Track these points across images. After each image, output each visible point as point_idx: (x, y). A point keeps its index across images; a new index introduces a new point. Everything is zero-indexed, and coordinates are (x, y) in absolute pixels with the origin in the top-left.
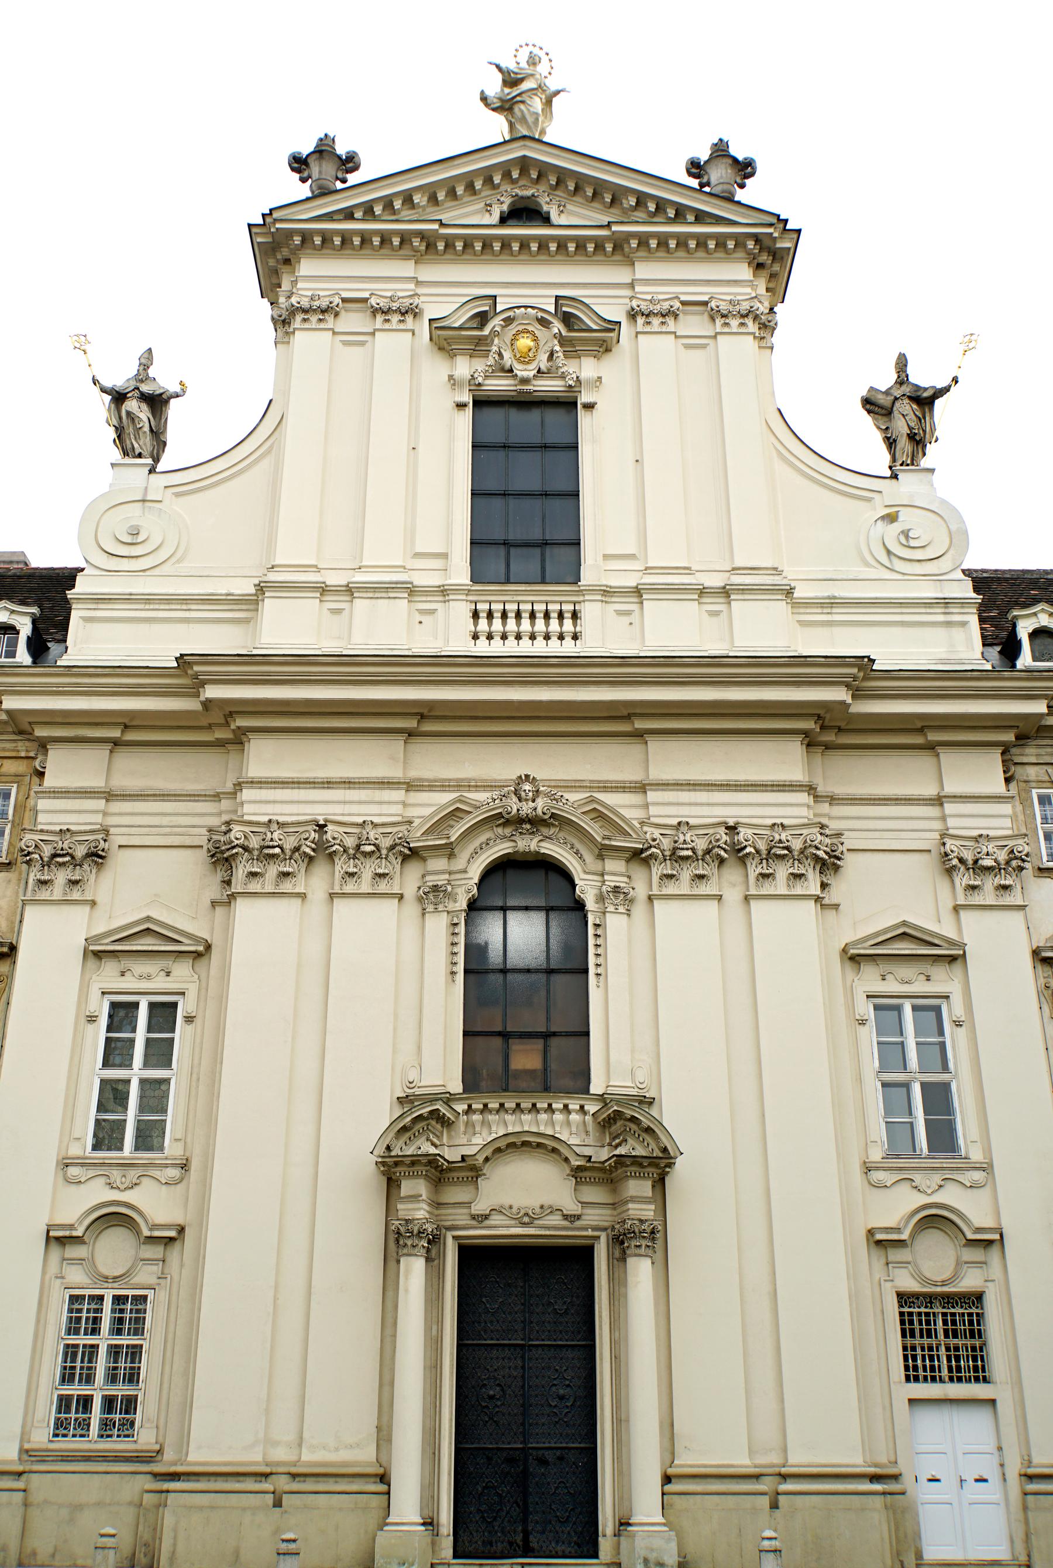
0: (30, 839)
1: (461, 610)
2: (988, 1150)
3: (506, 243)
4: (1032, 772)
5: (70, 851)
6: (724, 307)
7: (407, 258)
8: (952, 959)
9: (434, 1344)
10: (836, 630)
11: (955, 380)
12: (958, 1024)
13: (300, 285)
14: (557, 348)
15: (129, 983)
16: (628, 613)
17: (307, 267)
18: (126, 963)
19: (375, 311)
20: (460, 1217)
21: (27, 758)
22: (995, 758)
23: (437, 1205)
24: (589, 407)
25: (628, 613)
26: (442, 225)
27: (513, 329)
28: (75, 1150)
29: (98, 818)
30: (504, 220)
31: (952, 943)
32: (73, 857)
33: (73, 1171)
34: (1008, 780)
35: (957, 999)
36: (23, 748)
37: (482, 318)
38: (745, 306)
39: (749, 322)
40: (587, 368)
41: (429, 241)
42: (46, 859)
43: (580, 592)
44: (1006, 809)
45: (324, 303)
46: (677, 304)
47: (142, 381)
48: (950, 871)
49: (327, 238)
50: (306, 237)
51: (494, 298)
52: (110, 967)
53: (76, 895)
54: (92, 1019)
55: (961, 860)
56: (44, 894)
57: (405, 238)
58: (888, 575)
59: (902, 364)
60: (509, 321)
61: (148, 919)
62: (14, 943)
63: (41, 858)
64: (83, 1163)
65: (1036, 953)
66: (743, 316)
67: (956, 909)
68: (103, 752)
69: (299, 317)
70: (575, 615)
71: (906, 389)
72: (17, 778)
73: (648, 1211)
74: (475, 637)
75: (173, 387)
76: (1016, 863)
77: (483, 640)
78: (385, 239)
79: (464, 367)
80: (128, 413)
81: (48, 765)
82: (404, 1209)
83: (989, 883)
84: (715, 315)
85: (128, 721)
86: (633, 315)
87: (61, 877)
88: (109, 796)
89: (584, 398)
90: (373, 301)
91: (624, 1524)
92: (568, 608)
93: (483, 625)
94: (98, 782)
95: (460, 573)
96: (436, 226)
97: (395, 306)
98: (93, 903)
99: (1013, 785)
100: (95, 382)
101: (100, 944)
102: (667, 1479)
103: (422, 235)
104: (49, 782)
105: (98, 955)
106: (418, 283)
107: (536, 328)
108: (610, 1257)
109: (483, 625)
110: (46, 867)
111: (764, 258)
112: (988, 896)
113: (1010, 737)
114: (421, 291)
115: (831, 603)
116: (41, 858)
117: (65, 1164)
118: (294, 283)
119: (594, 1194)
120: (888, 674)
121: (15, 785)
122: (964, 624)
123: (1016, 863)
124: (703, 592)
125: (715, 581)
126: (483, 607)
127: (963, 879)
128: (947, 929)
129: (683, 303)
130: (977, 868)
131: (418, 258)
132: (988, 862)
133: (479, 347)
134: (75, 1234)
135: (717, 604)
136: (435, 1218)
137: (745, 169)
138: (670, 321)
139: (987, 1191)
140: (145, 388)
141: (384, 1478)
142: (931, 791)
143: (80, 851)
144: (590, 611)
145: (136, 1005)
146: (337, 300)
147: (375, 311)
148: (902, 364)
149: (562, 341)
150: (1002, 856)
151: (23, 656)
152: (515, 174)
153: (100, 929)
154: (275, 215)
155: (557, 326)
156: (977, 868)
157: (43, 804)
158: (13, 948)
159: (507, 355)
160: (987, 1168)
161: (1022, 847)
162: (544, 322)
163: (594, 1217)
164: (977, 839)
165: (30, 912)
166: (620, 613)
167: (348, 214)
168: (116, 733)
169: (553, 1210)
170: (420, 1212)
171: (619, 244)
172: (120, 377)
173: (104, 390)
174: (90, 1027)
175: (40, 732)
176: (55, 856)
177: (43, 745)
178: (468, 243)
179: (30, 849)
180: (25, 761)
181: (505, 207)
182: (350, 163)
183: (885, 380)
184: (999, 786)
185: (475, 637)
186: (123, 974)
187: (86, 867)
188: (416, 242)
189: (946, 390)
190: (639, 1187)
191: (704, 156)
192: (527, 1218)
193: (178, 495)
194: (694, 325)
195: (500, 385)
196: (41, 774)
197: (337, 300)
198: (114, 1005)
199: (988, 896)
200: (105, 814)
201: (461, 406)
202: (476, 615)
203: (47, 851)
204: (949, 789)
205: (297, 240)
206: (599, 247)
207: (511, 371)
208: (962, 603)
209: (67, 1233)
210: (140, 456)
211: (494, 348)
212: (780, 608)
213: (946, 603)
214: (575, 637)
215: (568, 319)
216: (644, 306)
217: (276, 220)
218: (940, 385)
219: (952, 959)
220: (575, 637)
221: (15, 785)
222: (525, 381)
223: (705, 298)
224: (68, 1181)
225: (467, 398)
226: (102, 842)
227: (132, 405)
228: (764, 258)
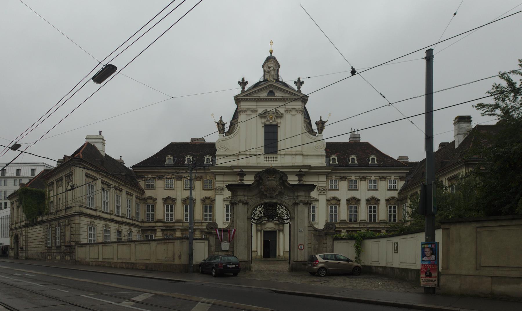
1: (262, 158)
2: (318, 221)
3: (268, 99)
4: (330, 177)
6: (298, 109)
7: (255, 101)
8: (317, 201)
9: (261, 240)
10: (308, 159)
11: (327, 121)
12: (317, 208)
13: (241, 106)
14: (275, 118)
16: (283, 157)
17: (242, 103)
19: (252, 111)
20: (264, 228)
22: (325, 176)
23: (261, 227)
24: (279, 127)
25: (283, 157)
26: (260, 97)
27: (269, 115)
28: (224, 221)
30: (268, 93)
31: (317, 199)
33: (224, 223)
34: (326, 179)
35: (317, 205)
37: (265, 113)
38: (300, 109)
39: (301, 112)
40: (279, 120)
41: (258, 99)
43: (278, 155)
44: (325, 183)
45: (244, 110)
46: (291, 109)
47: (221, 121)
48: (318, 190)
49: (244, 99)
50: (242, 99)
51: (267, 110)
52: (226, 202)
53: (221, 194)
54: (224, 207)
55: (320, 189)
56: (218, 193)
57: (255, 99)
58: (315, 151)
59: (321, 117)
60: (269, 113)
64: (225, 223)
65: (327, 200)
66: (300, 111)
67: (318, 195)
68: (222, 176)
69: (241, 112)
70: (277, 158)
71: (321, 122)
72: (212, 179)
73: (282, 228)
74: (265, 161)
75: (225, 123)
76: (325, 190)
77: (266, 161)
78: (252, 99)
79: (264, 120)
80: (220, 127)
82: (258, 228)
83: (322, 192)
84: (297, 111)
85: (225, 172)
86: (285, 111)
87: (219, 191)
88: (223, 182)
89: (279, 125)
90: (251, 109)
91: (279, 256)
92: (276, 157)
93: (266, 159)
94: (222, 180)
95: (263, 152)
96: (259, 97)
97: (254, 110)
98: (223, 194)
99: (327, 179)
100: (215, 122)
102: (284, 252)
103: (257, 98)
104: (217, 180)
105: (224, 200)
106: (257, 106)
107: (273, 115)
108: (278, 232)
109: (266, 159)
111: (304, 100)
112: (322, 194)
113: (327, 174)
114: (258, 107)
115: (307, 155)
117: (224, 223)
118: (240, 106)
119: (276, 226)
120: (313, 167)
122: (323, 158)
123: (325, 190)
124: (292, 155)
125: (294, 153)
126: (266, 157)
127: (320, 191)
128: (317, 197)
129: (292, 109)
130: (321, 190)
131: (257, 101)
132: (322, 189)
133: (265, 117)
135: (294, 156)
136: (261, 228)
137: (302, 83)
138: (290, 112)
139: (318, 226)
140: (222, 123)
141: (257, 252)
142: (317, 180)
143: (221, 188)
144: (279, 157)
145: (229, 206)
146: (246, 109)
147: (252, 111)
148: (321, 117)
149: (276, 116)
150: (324, 189)
151: (211, 163)
152: (270, 86)
154: (238, 96)
155: (275, 114)
156: (321, 190)
157: (216, 182)
158: (214, 200)
159: (269, 119)
160: (318, 223)
161: (326, 188)
162: (273, 113)
163: (277, 228)
164: (321, 187)
165: (216, 195)
166: (282, 157)
167: (247, 95)
168: (223, 174)
169: (273, 228)
170: (260, 228)
171: (284, 99)
172: (218, 120)
173: (216, 123)
174: (224, 208)
175: (215, 174)
177: (215, 175)
178: (263, 99)
181: (268, 92)
182: (247, 83)
183: (318, 120)
184: (325, 180)
185: (265, 161)
188: (256, 99)
189: (326, 122)
190: (281, 226)
191: (297, 81)
192: (270, 228)
193: (227, 140)
194: (294, 112)
195: (268, 123)
196: (215, 178)
197: (246, 109)
198: (226, 206)
199: (322, 194)
200: (223, 184)
201: (263, 127)
202: (265, 158)
204: (320, 180)
205: (240, 99)
206: (281, 99)
207: (269, 121)
208: (324, 155)
210: (222, 133)
211: (267, 118)
212: (301, 157)
213: (322, 155)
214: (277, 161)
215: (277, 112)
216: (287, 110)
217: (238, 97)
218: (325, 121)
219: (317, 201)
220: (277, 161)
222: (271, 123)
223: (295, 108)
224: (224, 224)
225: (263, 125)
227: (220, 125)
228: (304, 100)
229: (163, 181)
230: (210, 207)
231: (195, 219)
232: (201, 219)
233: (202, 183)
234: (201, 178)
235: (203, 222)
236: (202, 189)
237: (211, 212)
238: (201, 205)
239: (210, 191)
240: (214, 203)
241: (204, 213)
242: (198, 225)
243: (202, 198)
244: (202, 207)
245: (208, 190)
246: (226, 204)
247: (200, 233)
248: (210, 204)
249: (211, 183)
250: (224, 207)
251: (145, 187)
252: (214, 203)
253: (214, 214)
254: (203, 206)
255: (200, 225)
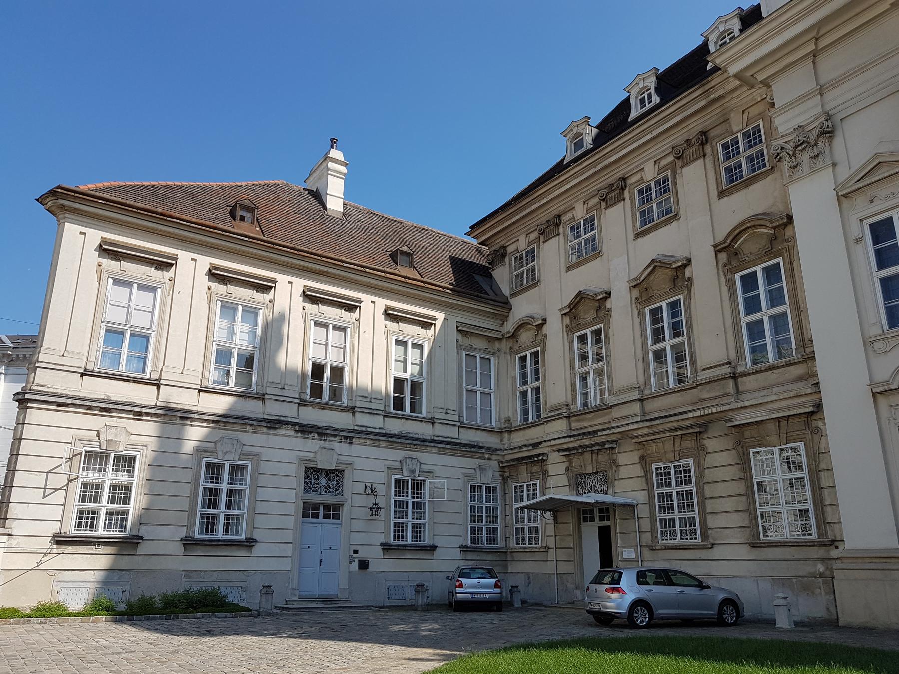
0: (776, 143)
5: (804, 139)
15: (877, 206)
18: (871, 192)
21: (762, 100)
29: (819, 109)
32: (808, 143)
36: (758, 93)
42: (791, 153)
52: (860, 201)
54: (858, 240)
61: (876, 155)
62: (790, 214)
63: (788, 154)
81: (774, 97)
87: (804, 157)
101: (845, 189)
110: (793, 158)
116: (788, 154)
117: (868, 343)
121: (761, 120)
134: (892, 387)
153: (841, 178)
158: (790, 218)
168: (811, 47)
175: (761, 77)
176: (796, 147)
177: (766, 84)
179: (778, 151)
180: (762, 102)
186: (871, 201)
187: (820, 144)
198: (871, 226)
203: (790, 147)
209: (886, 388)
221: (761, 120)
226: (824, 122)
229: (561, 236)
230: (772, 274)
231: (700, 364)
232: (733, 355)
233: (709, 165)
234: (703, 144)
235: (740, 370)
236: (714, 193)
237: (784, 303)
238: (723, 279)
239: (757, 188)
240: (787, 241)
241: (745, 319)
242: (716, 398)
243: (720, 237)
244: (725, 289)
245: (747, 186)
246: (861, 215)
247: (728, 443)
248: (770, 253)
249: (761, 141)
250: (858, 240)
251: (511, 289)
252: (787, 241)
253: (799, 309)
254: (731, 284)
255: (727, 395)
